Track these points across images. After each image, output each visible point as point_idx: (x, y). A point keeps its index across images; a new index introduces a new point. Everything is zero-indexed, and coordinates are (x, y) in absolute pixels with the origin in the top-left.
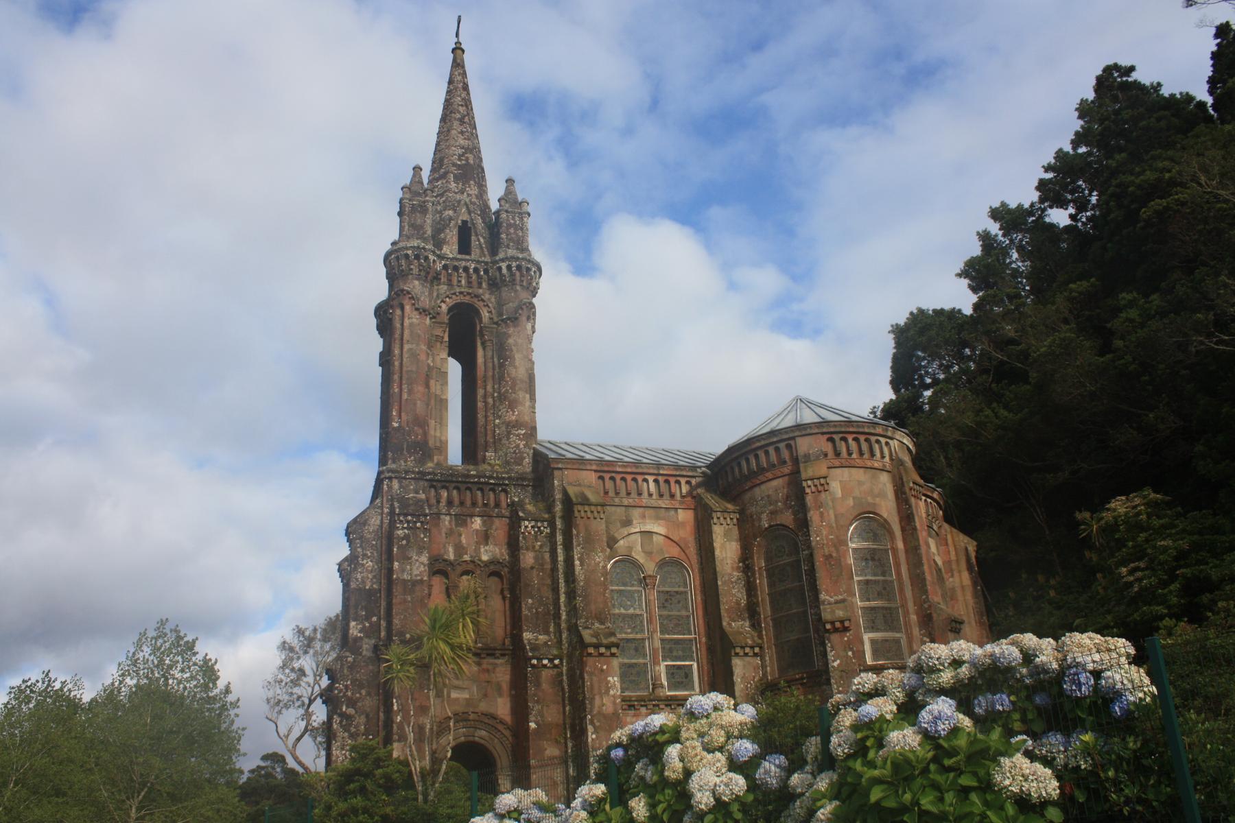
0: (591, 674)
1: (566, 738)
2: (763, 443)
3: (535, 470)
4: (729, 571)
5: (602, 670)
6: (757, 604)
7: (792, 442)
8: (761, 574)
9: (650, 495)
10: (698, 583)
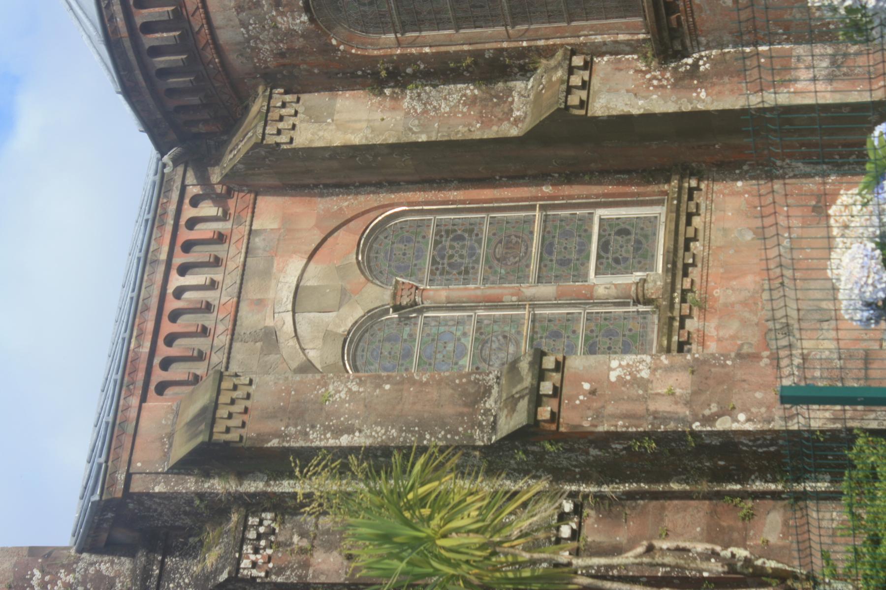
0: (598, 416)
1: (744, 495)
3: (129, 551)
4: (399, 116)
5: (593, 392)
6: (478, 55)
8: (412, 44)
9: (213, 285)
10: (419, 196)
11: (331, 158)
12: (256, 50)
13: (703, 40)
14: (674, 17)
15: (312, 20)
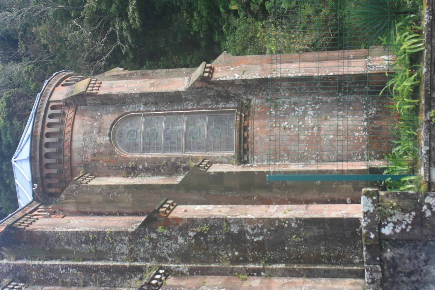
2: (40, 124)
7: (51, 104)
11: (100, 194)
12: (85, 152)
13: (255, 157)
14: (246, 144)
15: (110, 140)
